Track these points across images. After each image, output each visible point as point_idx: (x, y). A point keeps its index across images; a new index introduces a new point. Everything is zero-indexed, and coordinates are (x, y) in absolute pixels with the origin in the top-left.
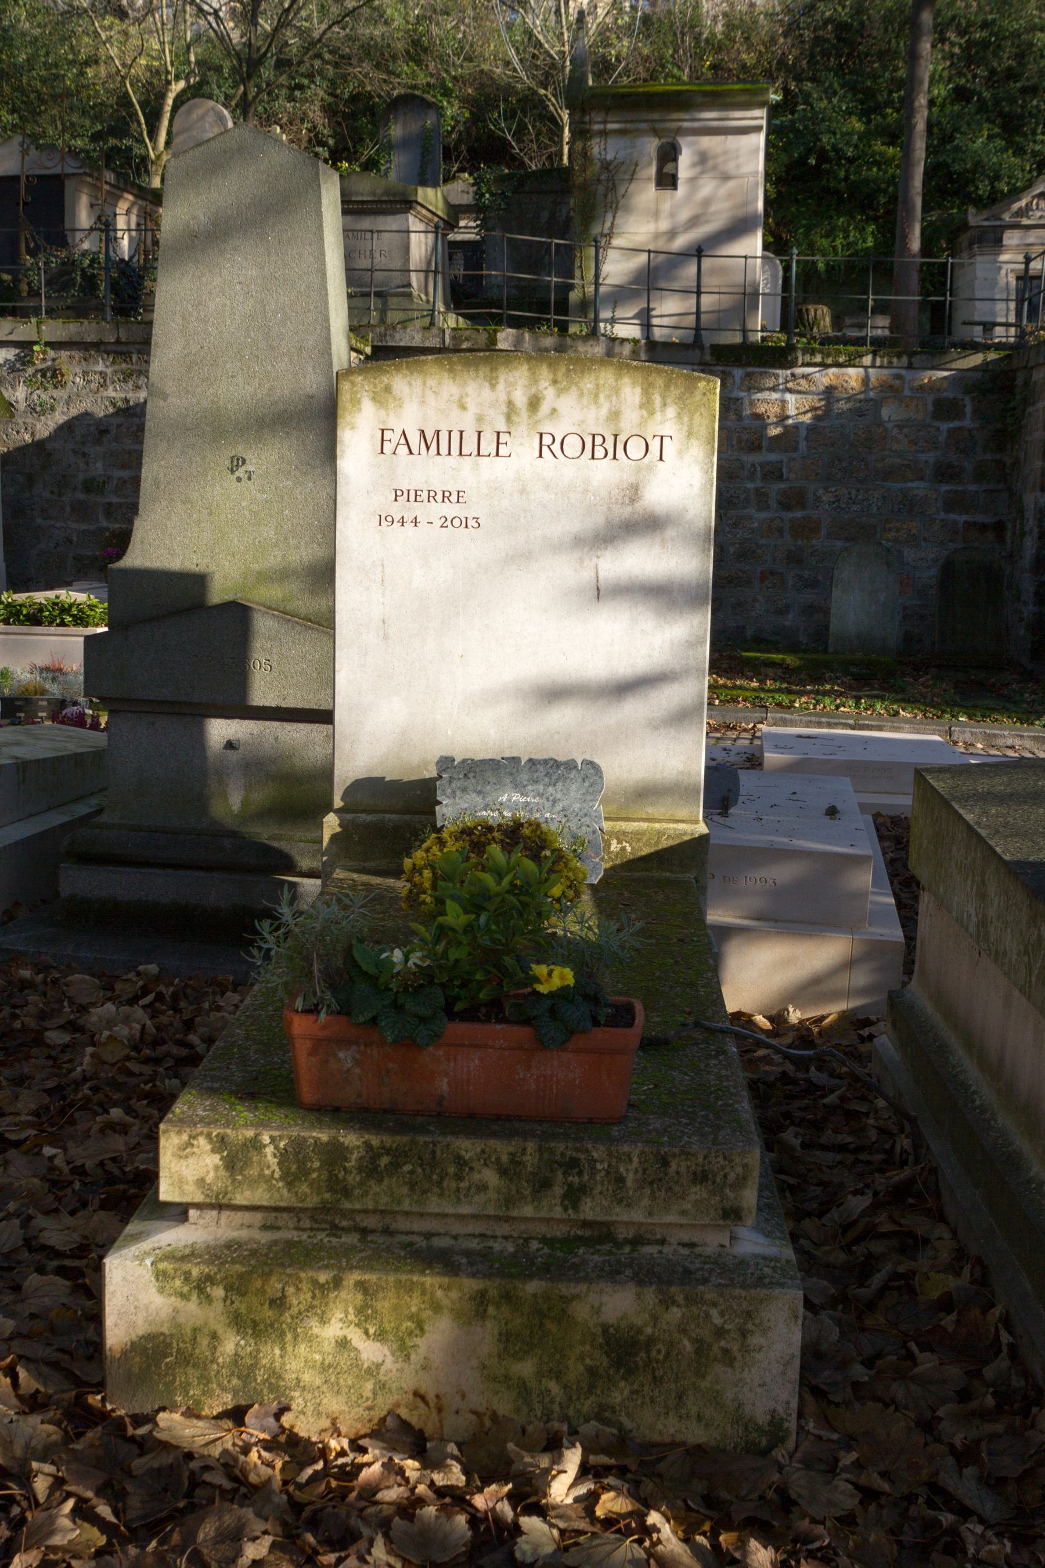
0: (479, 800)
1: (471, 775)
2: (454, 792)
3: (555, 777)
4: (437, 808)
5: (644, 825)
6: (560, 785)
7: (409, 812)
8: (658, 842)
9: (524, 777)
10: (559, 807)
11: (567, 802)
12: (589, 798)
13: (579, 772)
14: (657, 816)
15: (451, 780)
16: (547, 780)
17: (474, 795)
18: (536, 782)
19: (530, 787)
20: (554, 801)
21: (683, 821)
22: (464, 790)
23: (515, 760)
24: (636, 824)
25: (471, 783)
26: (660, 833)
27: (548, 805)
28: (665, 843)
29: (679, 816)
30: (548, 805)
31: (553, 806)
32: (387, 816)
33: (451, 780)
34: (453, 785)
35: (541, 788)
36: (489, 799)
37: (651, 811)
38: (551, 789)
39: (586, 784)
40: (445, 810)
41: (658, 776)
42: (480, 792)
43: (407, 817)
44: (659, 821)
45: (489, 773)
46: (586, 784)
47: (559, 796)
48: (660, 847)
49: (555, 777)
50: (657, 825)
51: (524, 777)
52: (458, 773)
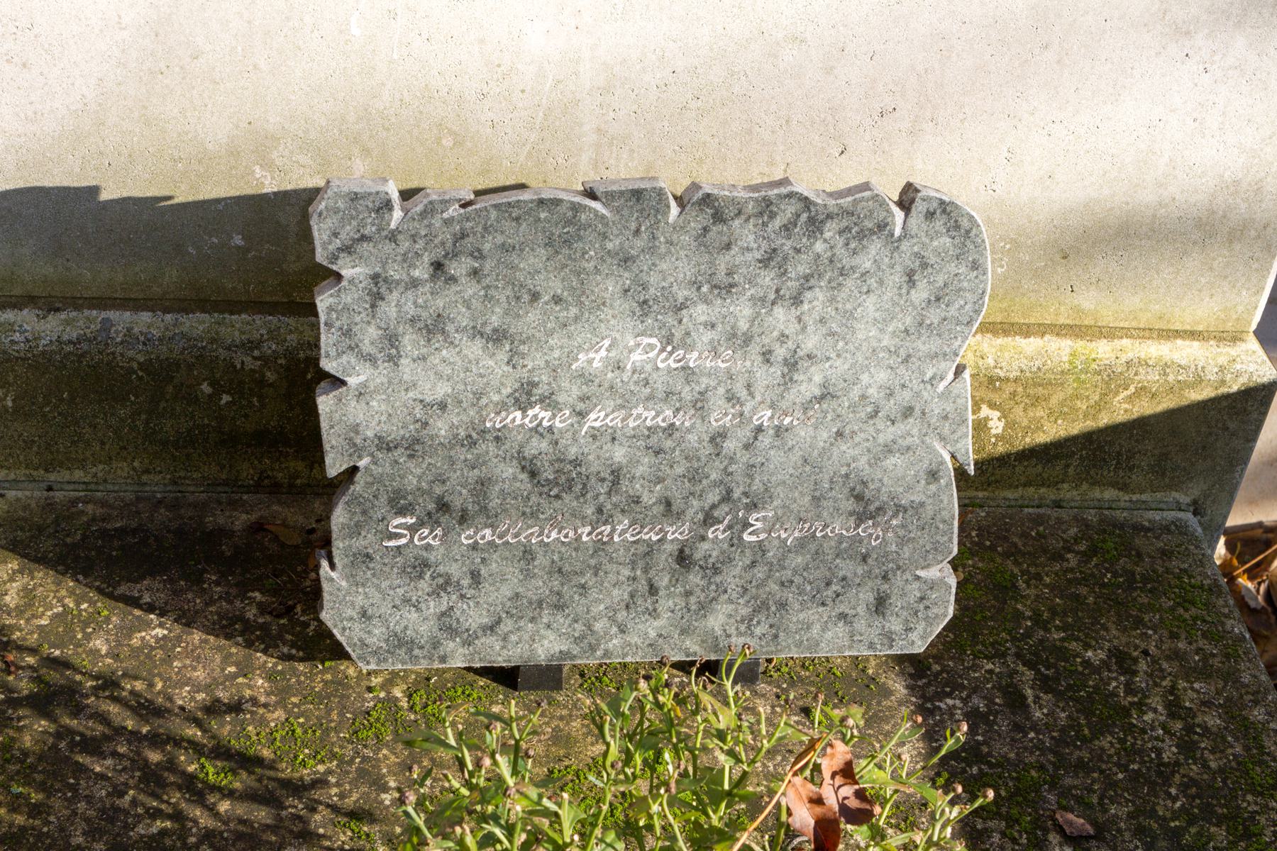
0: (495, 369)
1: (459, 268)
2: (392, 339)
3: (800, 267)
4: (325, 403)
5: (1060, 349)
6: (817, 300)
7: (203, 304)
8: (1098, 407)
9: (675, 269)
10: (808, 384)
11: (840, 367)
12: (924, 346)
13: (894, 244)
14: (1107, 319)
15: (378, 288)
16: (767, 279)
17: (474, 348)
18: (726, 289)
19: (700, 312)
20: (791, 365)
21: (1193, 335)
22: (434, 328)
23: (641, 200)
24: (1031, 345)
25: (459, 300)
26: (1112, 379)
27: (766, 377)
28: (1122, 410)
29: (1185, 316)
30: (766, 377)
31: (788, 380)
32: (121, 319)
33: (378, 288)
34: (389, 309)
35: (742, 311)
36: (535, 361)
37: (1090, 302)
38: (781, 317)
39: (920, 294)
40: (355, 411)
41: (1147, 196)
42: (497, 337)
43: (197, 324)
44: (1110, 333)
45: (535, 259)
46: (920, 294)
47: (810, 343)
48: (1104, 420)
49: (800, 267)
50: (1103, 350)
51: (675, 269)
52: (408, 260)
